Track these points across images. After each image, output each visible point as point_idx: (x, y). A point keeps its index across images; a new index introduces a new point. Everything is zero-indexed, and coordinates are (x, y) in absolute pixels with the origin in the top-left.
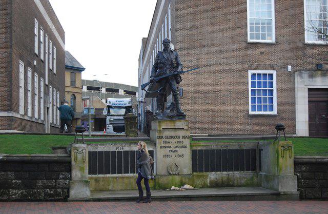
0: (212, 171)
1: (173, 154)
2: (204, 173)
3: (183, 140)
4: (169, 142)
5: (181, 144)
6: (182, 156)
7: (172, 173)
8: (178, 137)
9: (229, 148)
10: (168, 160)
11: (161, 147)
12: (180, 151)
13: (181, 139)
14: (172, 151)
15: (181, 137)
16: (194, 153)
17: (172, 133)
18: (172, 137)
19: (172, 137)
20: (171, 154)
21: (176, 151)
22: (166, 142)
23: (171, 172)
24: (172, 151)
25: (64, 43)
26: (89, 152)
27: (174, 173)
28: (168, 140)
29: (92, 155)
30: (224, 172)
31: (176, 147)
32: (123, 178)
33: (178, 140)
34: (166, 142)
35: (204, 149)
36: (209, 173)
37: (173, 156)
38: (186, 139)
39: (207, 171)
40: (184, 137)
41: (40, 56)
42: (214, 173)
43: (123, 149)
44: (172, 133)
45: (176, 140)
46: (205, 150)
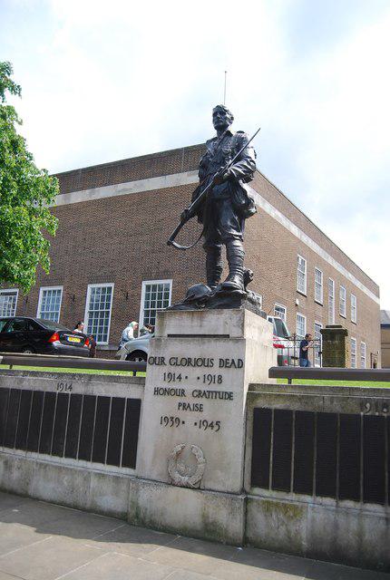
0: (321, 493)
1: (190, 417)
2: (292, 497)
3: (223, 372)
4: (180, 378)
5: (214, 387)
6: (215, 425)
7: (177, 481)
8: (203, 362)
10: (178, 433)
11: (157, 391)
12: (210, 409)
13: (216, 370)
14: (185, 406)
15: (216, 363)
17: (193, 350)
18: (188, 362)
19: (188, 362)
20: (182, 414)
21: (199, 408)
22: (170, 377)
23: (177, 476)
24: (185, 406)
25: (378, 296)
27: (185, 479)
28: (173, 370)
30: (369, 506)
32: (60, 469)
33: (207, 371)
34: (170, 377)
35: (295, 406)
36: (308, 498)
38: (233, 371)
39: (303, 488)
41: (312, 296)
42: (328, 501)
43: (70, 388)
44: (193, 350)
45: (199, 371)
46: (298, 413)
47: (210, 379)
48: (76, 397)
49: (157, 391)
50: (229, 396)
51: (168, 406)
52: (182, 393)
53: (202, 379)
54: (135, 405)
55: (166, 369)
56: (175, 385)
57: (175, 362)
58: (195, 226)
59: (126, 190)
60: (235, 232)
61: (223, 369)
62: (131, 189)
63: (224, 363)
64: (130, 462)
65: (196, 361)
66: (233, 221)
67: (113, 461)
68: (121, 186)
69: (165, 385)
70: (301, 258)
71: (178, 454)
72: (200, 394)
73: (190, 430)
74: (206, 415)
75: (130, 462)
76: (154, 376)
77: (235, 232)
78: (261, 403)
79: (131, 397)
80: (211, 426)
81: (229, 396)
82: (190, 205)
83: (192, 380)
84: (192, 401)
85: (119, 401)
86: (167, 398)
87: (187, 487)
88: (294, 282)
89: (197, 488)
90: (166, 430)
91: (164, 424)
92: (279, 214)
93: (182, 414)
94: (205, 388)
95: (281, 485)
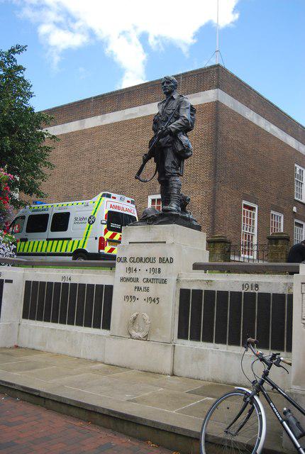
1: (142, 295)
3: (162, 266)
4: (135, 270)
5: (158, 276)
6: (155, 300)
8: (148, 260)
9: (262, 290)
10: (135, 304)
12: (154, 289)
13: (157, 265)
14: (138, 289)
15: (157, 260)
16: (184, 294)
18: (141, 260)
19: (141, 260)
20: (137, 294)
21: (147, 290)
24: (138, 289)
26: (28, 283)
28: (134, 266)
29: (33, 289)
31: (148, 281)
35: (204, 288)
37: (141, 299)
40: (162, 260)
43: (70, 279)
44: (144, 252)
45: (148, 266)
47: (154, 270)
48: (74, 285)
49: (122, 279)
50: (164, 281)
51: (129, 288)
52: (137, 280)
53: (149, 271)
54: (110, 289)
55: (128, 264)
56: (133, 275)
57: (133, 260)
58: (152, 164)
59: (132, 114)
60: (174, 171)
61: (162, 264)
62: (136, 113)
63: (162, 260)
64: (107, 326)
65: (146, 259)
66: (173, 162)
67: (97, 326)
68: (128, 111)
69: (127, 275)
70: (298, 168)
71: (135, 319)
72: (148, 281)
73: (141, 307)
74: (151, 294)
75: (107, 326)
76: (120, 267)
77: (174, 171)
78: (185, 286)
79: (107, 284)
80: (154, 301)
81: (164, 281)
82: (146, 150)
83: (143, 271)
84: (141, 284)
85: (100, 287)
86: (128, 283)
87: (139, 339)
88: (291, 191)
89: (146, 338)
90: (128, 304)
91: (126, 300)
92: (273, 127)
93: (137, 294)
94: (151, 276)
95: (195, 338)
